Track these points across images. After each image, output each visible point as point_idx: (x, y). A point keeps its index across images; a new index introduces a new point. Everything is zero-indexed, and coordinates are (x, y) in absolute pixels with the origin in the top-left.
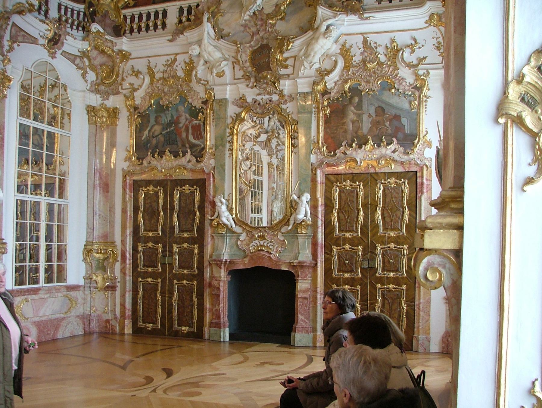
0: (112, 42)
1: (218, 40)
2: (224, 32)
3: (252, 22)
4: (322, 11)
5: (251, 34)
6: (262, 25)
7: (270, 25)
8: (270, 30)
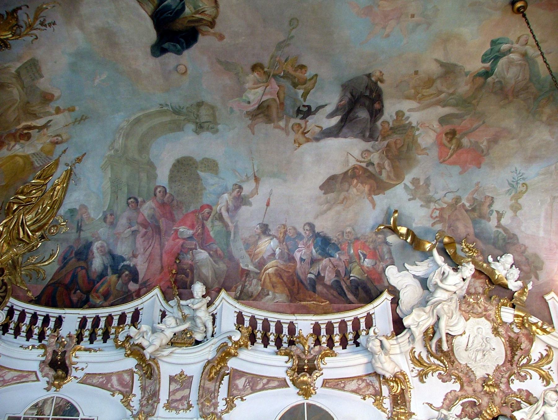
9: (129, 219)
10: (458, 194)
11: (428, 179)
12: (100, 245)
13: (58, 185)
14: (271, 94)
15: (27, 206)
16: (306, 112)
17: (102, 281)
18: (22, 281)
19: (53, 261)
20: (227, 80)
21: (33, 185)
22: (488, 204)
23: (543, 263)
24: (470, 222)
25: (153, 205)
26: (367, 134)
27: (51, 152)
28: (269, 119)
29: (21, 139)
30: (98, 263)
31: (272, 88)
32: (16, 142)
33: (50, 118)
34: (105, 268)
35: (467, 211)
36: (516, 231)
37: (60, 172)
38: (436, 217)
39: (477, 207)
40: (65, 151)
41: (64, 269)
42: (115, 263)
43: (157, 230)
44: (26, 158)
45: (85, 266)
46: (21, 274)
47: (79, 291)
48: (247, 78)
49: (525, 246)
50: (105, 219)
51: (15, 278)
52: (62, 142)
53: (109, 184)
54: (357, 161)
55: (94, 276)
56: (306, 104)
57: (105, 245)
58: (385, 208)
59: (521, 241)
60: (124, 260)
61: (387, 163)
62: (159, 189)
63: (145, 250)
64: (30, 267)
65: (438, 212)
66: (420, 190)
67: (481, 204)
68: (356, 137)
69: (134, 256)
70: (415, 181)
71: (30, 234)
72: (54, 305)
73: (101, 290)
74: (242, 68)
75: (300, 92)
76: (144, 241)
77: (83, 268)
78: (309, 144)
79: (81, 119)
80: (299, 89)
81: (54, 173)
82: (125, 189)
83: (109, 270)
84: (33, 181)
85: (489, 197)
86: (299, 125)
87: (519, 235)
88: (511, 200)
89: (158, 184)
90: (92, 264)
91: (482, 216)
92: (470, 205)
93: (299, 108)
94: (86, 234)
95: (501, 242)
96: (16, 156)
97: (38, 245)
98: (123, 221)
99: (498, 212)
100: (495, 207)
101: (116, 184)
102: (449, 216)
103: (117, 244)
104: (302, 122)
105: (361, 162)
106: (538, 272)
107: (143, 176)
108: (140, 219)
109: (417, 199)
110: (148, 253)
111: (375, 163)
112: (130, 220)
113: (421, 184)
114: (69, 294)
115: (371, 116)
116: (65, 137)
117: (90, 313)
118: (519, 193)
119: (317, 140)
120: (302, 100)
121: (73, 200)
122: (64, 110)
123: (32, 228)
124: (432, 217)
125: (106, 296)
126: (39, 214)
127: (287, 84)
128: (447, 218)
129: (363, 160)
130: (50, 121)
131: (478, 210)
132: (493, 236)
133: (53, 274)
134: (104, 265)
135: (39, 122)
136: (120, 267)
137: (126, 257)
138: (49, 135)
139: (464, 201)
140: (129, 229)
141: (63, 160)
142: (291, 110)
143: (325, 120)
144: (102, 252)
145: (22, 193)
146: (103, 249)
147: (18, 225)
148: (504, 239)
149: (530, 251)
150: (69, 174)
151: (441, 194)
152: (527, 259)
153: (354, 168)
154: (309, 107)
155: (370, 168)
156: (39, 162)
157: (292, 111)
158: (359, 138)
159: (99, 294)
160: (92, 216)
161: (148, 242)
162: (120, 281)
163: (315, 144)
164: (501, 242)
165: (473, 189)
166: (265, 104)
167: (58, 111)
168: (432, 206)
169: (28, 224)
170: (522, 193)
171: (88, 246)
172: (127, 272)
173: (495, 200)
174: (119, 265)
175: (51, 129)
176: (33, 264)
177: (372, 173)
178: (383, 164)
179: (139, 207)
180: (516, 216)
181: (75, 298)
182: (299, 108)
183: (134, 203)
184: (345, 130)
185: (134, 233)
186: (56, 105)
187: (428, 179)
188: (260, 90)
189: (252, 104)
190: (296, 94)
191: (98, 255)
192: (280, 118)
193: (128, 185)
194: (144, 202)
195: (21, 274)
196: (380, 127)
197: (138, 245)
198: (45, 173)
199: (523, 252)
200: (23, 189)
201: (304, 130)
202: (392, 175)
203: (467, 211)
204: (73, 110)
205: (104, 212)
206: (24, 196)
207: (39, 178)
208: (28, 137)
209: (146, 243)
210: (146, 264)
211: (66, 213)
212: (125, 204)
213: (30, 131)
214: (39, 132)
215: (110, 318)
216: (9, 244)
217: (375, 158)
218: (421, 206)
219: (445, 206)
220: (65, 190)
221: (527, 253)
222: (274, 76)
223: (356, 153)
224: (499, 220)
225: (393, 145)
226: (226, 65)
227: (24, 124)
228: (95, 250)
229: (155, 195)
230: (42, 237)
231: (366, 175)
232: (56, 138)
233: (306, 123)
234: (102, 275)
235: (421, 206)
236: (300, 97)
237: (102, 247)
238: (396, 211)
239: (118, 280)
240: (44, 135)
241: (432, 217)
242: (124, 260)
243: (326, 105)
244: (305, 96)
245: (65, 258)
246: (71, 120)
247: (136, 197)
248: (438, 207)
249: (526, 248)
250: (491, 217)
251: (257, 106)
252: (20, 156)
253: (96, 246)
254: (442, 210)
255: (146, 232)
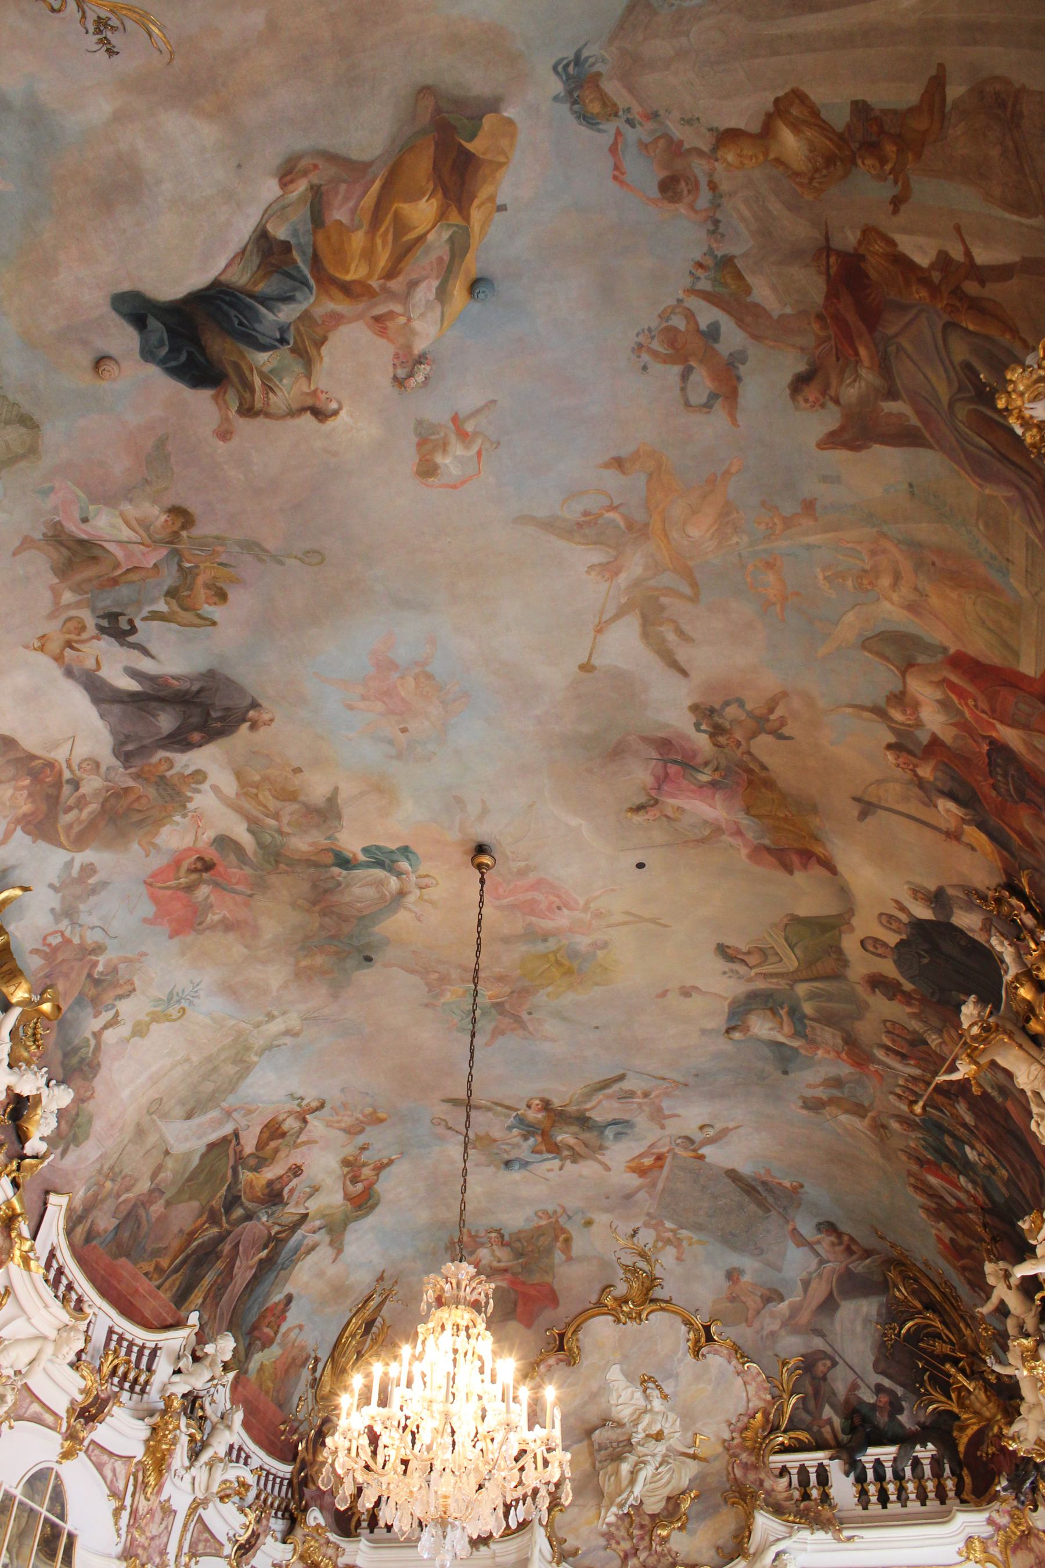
0: (338, 1547)
1: (558, 1563)
2: (566, 1546)
3: (622, 1529)
4: (764, 1523)
5: (622, 1554)
6: (642, 1538)
7: (658, 1539)
8: (659, 1549)
10: (108, 942)
11: (104, 884)
14: (129, 555)
16: (117, 628)
20: (120, 467)
22: (119, 991)
23: (87, 1138)
24: (76, 994)
26: (130, 747)
28: (63, 570)
31: (143, 554)
35: (90, 975)
36: (105, 1060)
38: (49, 945)
39: (105, 984)
48: (147, 504)
49: (94, 1092)
54: (68, 762)
56: (138, 623)
58: (11, 862)
59: (98, 1083)
61: (94, 806)
65: (59, 939)
66: (79, 887)
67: (115, 985)
68: (113, 732)
70: (89, 870)
74: (166, 489)
75: (162, 606)
78: (52, 665)
80: (167, 603)
85: (132, 984)
86: (83, 628)
87: (103, 1072)
88: (148, 1014)
91: (95, 1001)
92: (101, 973)
93: (121, 614)
95: (75, 1061)
99: (117, 1014)
100: (124, 1007)
102: (63, 961)
104: (91, 630)
105: (69, 767)
106: (72, 1146)
109: (60, 895)
111: (82, 791)
113: (90, 881)
115: (171, 736)
118: (165, 1015)
119: (69, 673)
120: (144, 613)
124: (45, 939)
127: (169, 578)
128: (59, 960)
129: (75, 767)
131: (102, 988)
132: (76, 1041)
139: (102, 960)
142: (108, 602)
143: (119, 667)
148: (82, 1060)
149: (90, 1106)
151: (94, 920)
152: (77, 1115)
153: (51, 765)
154: (133, 630)
155: (66, 789)
157: (107, 602)
158: (115, 739)
163: (57, 672)
164: (75, 1061)
165: (129, 955)
166: (96, 552)
168: (64, 925)
170: (168, 1018)
173: (132, 996)
177: (58, 797)
178: (86, 804)
180: (128, 1041)
182: (121, 614)
184: (116, 709)
187: (104, 884)
188: (126, 534)
189: (84, 526)
190: (153, 601)
192: (77, 589)
196: (155, 759)
199: (83, 1101)
201: (77, 642)
202: (76, 829)
203: (90, 975)
217: (92, 784)
218: (52, 910)
219: (76, 941)
221: (85, 1105)
222: (176, 552)
223: (82, 750)
224: (105, 1027)
225: (133, 797)
226: (158, 457)
231: (51, 791)
233: (93, 638)
235: (52, 910)
236: (150, 609)
238: (26, 889)
241: (45, 939)
243: (153, 657)
244: (155, 616)
248: (67, 934)
249: (92, 1096)
250: (104, 1013)
251: (85, 537)
254: (67, 942)
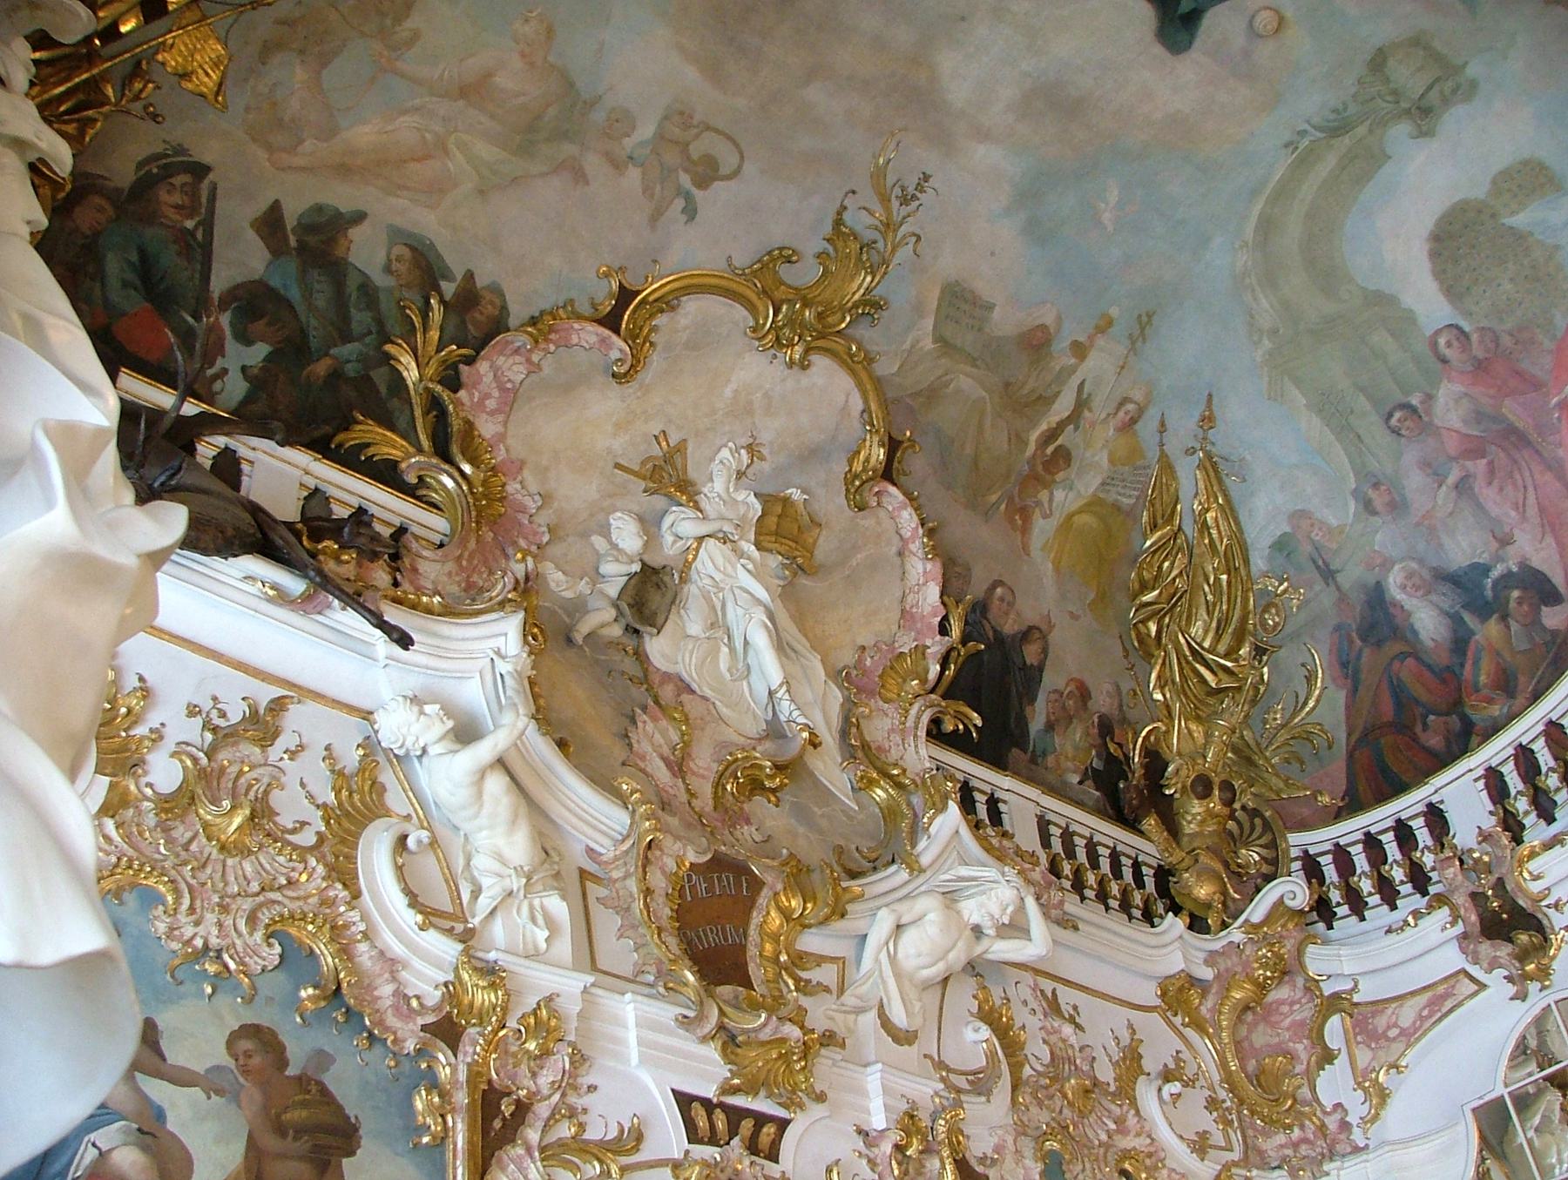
9: (1425, 464)
12: (1403, 574)
13: (1207, 510)
15: (1175, 606)
17: (1469, 654)
18: (1286, 781)
19: (1324, 688)
21: (1155, 552)
25: (1459, 388)
27: (1136, 452)
29: (1054, 474)
30: (1427, 621)
32: (1048, 485)
33: (1074, 382)
34: (1456, 620)
37: (1189, 478)
40: (1163, 424)
41: (1362, 691)
42: (1469, 590)
43: (1514, 438)
44: (1094, 505)
45: (1405, 649)
46: (1273, 766)
47: (1432, 717)
50: (1368, 507)
51: (1266, 784)
52: (1141, 411)
53: (1316, 421)
55: (1443, 658)
57: (1414, 565)
60: (1485, 570)
62: (1442, 341)
63: (1520, 508)
64: (1280, 739)
69: (1505, 541)
71: (1229, 664)
72: (1400, 788)
73: (1483, 679)
76: (1501, 489)
77: (1403, 656)
79: (1143, 329)
81: (1177, 490)
82: (1362, 402)
83: (1467, 617)
84: (1148, 543)
89: (1428, 333)
90: (1415, 633)
94: (1352, 575)
96: (1070, 516)
97: (1262, 675)
98: (1415, 482)
101: (1330, 409)
103: (1441, 545)
107: (1380, 339)
108: (1452, 445)
110: (1532, 511)
112: (1429, 465)
114: (1415, 739)
116: (1138, 395)
117: (1497, 750)
121: (1264, 518)
122: (1091, 338)
123: (1222, 648)
125: (1506, 684)
126: (1215, 605)
130: (1082, 383)
133: (1342, 718)
134: (1447, 614)
135: (1063, 407)
136: (1489, 593)
137: (1484, 558)
138: (1103, 416)
140: (1444, 488)
141: (1174, 447)
144: (1417, 588)
145: (1144, 587)
146: (1416, 580)
147: (1188, 662)
150: (1212, 468)
156: (1128, 492)
159: (1485, 692)
160: (1334, 522)
161: (1515, 485)
162: (1514, 627)
167: (1079, 350)
169: (1206, 644)
171: (1376, 598)
172: (1516, 594)
174: (1481, 587)
175: (1097, 403)
176: (1283, 726)
179: (1426, 419)
181: (1434, 741)
183: (1408, 417)
185: (1463, 487)
186: (1066, 343)
191: (1415, 601)
193: (1362, 390)
194: (1429, 398)
195: (1273, 766)
197: (1495, 511)
198: (1158, 506)
200: (1139, 575)
204: (1110, 323)
205: (1355, 493)
206: (1154, 589)
207: (1154, 527)
208: (1063, 457)
209: (1509, 489)
210: (1549, 540)
211: (1270, 559)
212: (1389, 438)
213: (1059, 442)
214: (1076, 429)
215: (1553, 729)
216: (1198, 719)
220: (1229, 510)
227: (1034, 436)
228: (1399, 596)
229: (1444, 361)
230: (1259, 651)
232: (1121, 414)
234: (1460, 642)
237: (1410, 575)
239: (1508, 627)
240: (1093, 425)
242: (1485, 570)
245: (1344, 665)
246: (1121, 350)
247: (1404, 400)
252: (1080, 511)
253: (1394, 584)
255: (1491, 463)
